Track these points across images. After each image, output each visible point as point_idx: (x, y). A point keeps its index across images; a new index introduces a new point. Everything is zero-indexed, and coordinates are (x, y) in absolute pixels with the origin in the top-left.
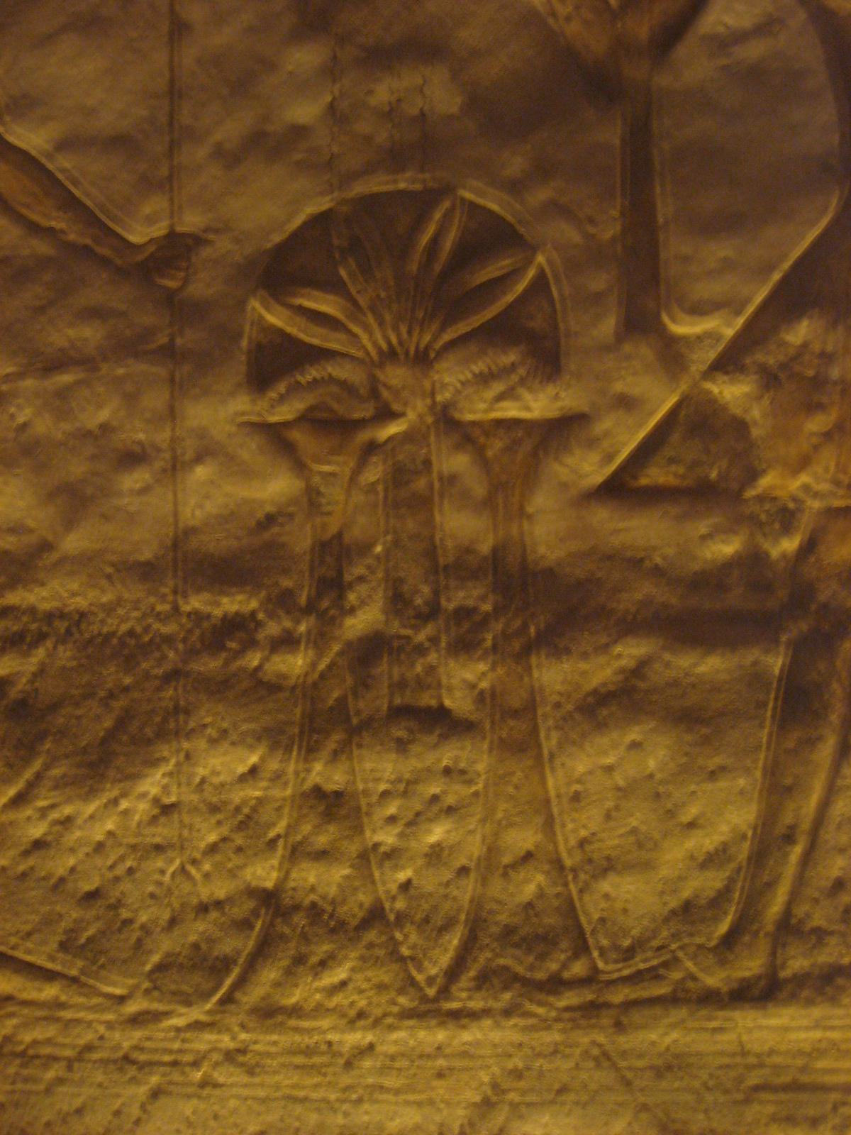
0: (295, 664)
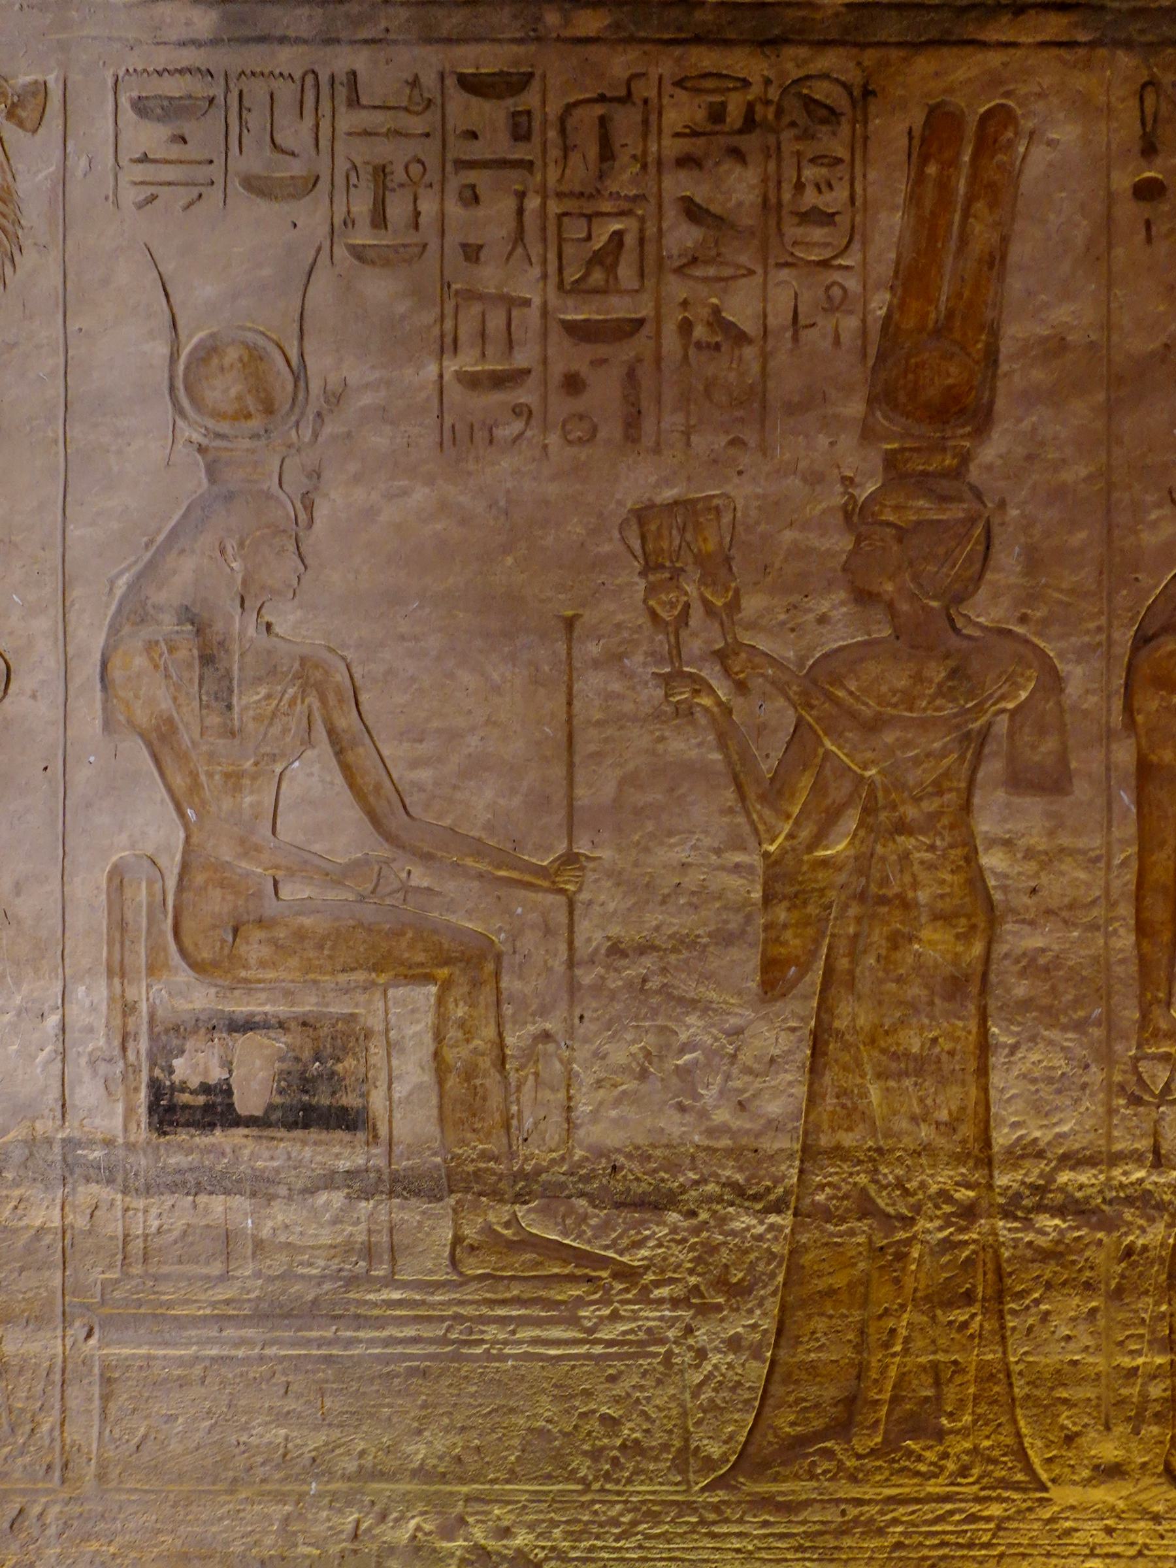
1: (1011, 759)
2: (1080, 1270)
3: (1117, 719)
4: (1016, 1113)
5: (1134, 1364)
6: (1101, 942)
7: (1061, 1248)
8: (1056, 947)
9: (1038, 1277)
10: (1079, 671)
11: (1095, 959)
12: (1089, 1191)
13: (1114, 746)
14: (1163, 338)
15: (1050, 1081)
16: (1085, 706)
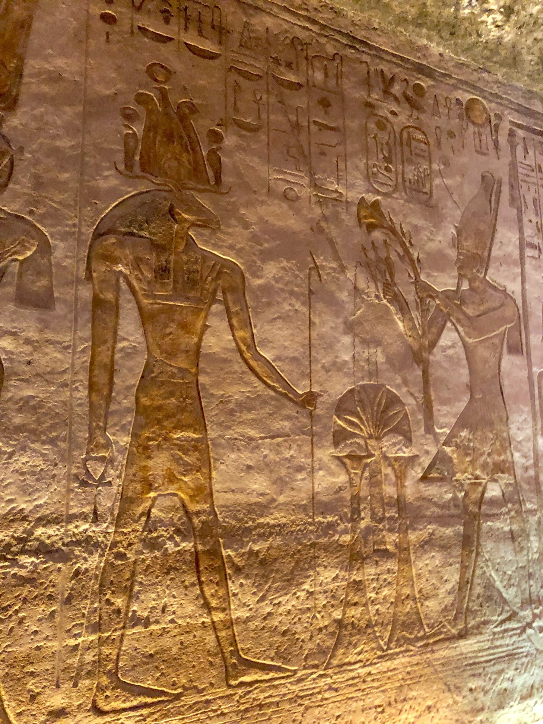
0: (347, 538)
1: (19, 287)
2: (45, 588)
3: (82, 274)
4: (11, 494)
5: (77, 643)
6: (68, 394)
7: (35, 575)
8: (41, 395)
9: (19, 595)
10: (62, 245)
11: (64, 403)
12: (54, 539)
13: (80, 287)
14: (113, 90)
15: (34, 474)
16: (65, 264)
